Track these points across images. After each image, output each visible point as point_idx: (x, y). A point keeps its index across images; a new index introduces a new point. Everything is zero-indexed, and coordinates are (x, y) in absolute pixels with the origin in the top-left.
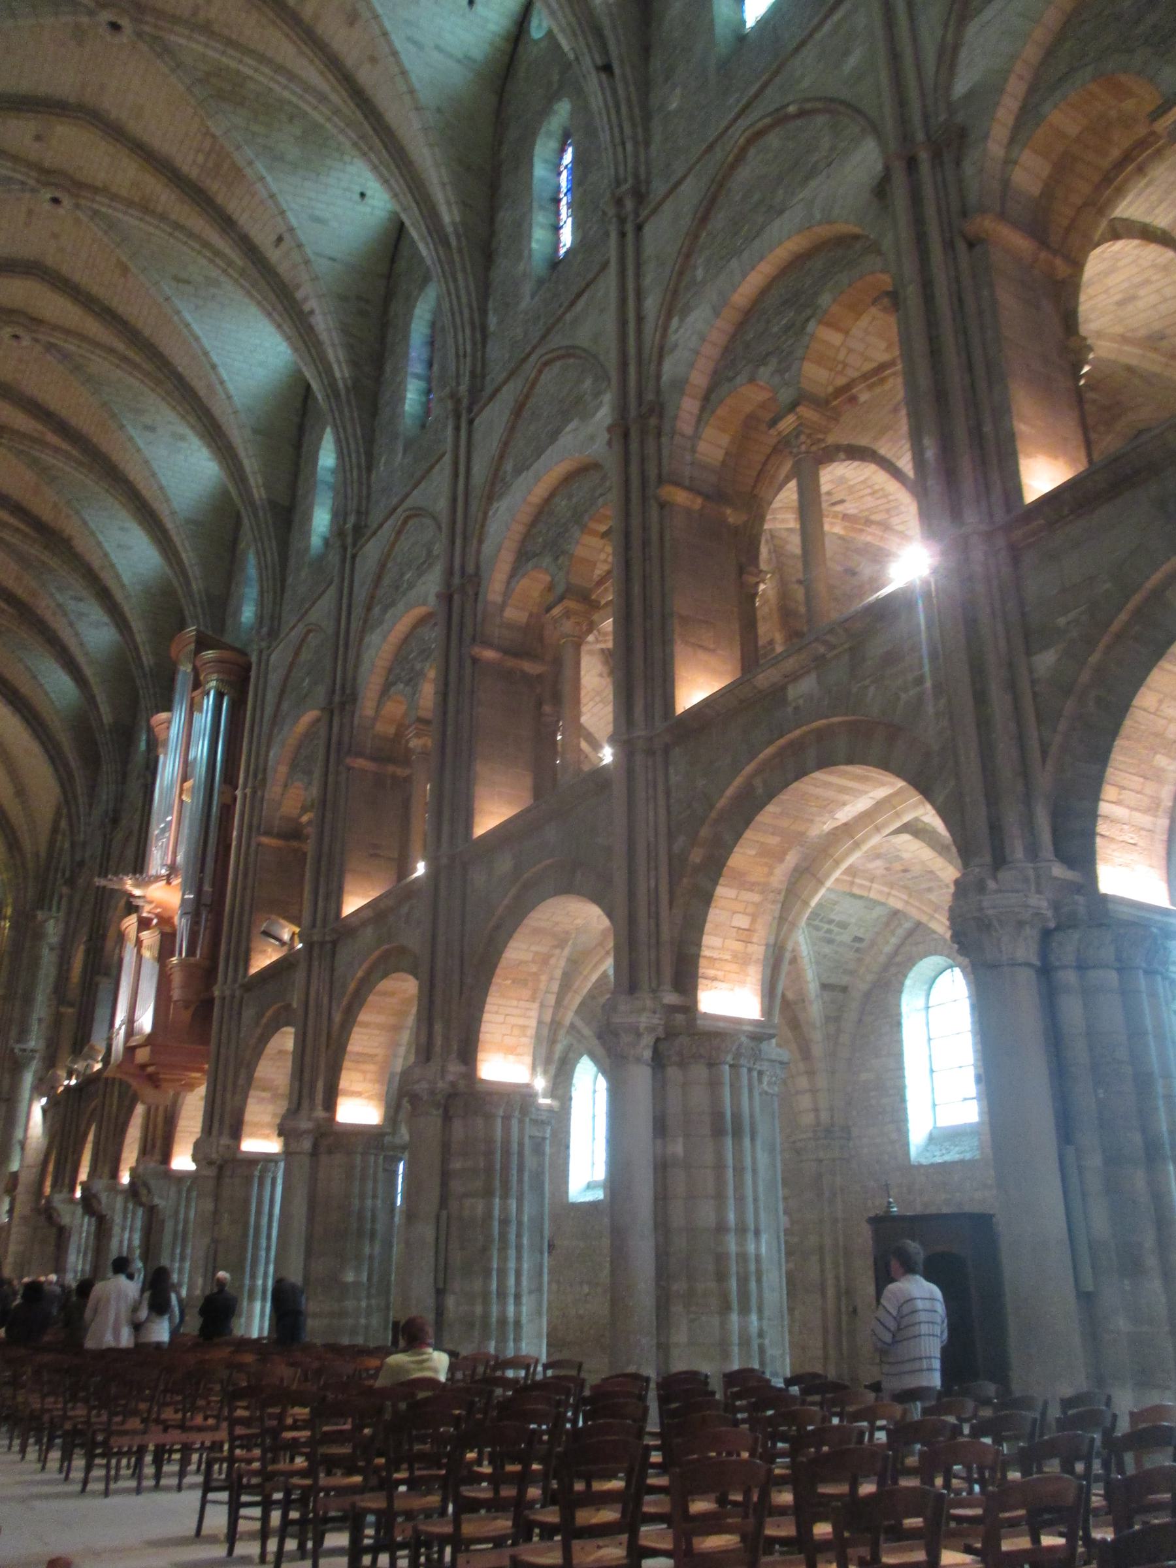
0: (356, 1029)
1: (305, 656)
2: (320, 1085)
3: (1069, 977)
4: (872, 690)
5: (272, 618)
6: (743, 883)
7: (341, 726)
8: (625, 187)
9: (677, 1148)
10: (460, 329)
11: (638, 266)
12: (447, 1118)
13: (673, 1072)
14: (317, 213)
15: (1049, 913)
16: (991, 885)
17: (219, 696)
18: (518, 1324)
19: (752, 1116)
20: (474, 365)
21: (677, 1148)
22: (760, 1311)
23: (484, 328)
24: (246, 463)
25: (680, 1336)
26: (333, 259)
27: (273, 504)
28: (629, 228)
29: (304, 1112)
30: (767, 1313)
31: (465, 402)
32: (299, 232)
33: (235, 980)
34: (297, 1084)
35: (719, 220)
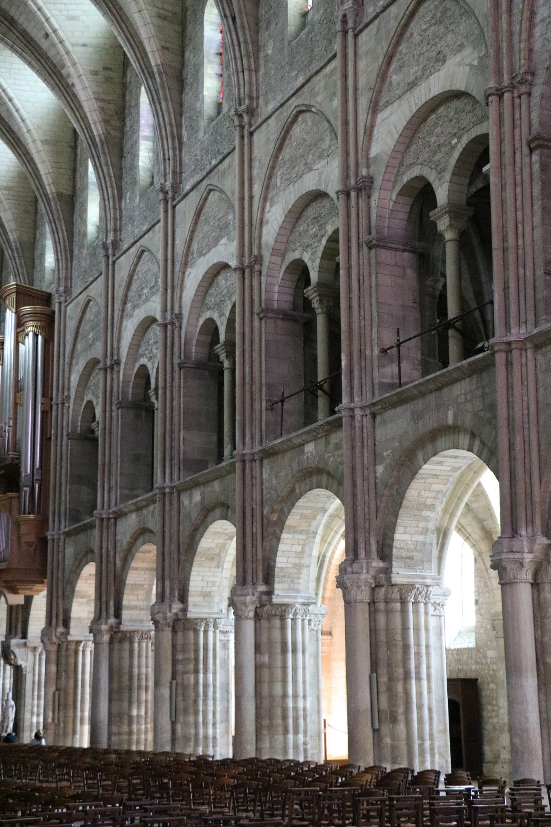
0: (130, 572)
1: (89, 316)
2: (112, 603)
3: (381, 606)
4: (331, 459)
5: (66, 278)
6: (294, 530)
7: (112, 379)
8: (243, 107)
9: (266, 659)
10: (165, 140)
11: (251, 160)
12: (174, 632)
13: (264, 623)
14: (71, 13)
15: (372, 581)
16: (349, 569)
17: (36, 335)
18: (214, 738)
19: (303, 642)
20: (175, 166)
21: (266, 659)
22: (305, 732)
24: (40, 166)
25: (266, 745)
26: (85, 45)
27: (60, 196)
28: (246, 134)
29: (103, 620)
30: (309, 734)
32: (60, 32)
33: (59, 529)
34: (99, 603)
35: (287, 153)
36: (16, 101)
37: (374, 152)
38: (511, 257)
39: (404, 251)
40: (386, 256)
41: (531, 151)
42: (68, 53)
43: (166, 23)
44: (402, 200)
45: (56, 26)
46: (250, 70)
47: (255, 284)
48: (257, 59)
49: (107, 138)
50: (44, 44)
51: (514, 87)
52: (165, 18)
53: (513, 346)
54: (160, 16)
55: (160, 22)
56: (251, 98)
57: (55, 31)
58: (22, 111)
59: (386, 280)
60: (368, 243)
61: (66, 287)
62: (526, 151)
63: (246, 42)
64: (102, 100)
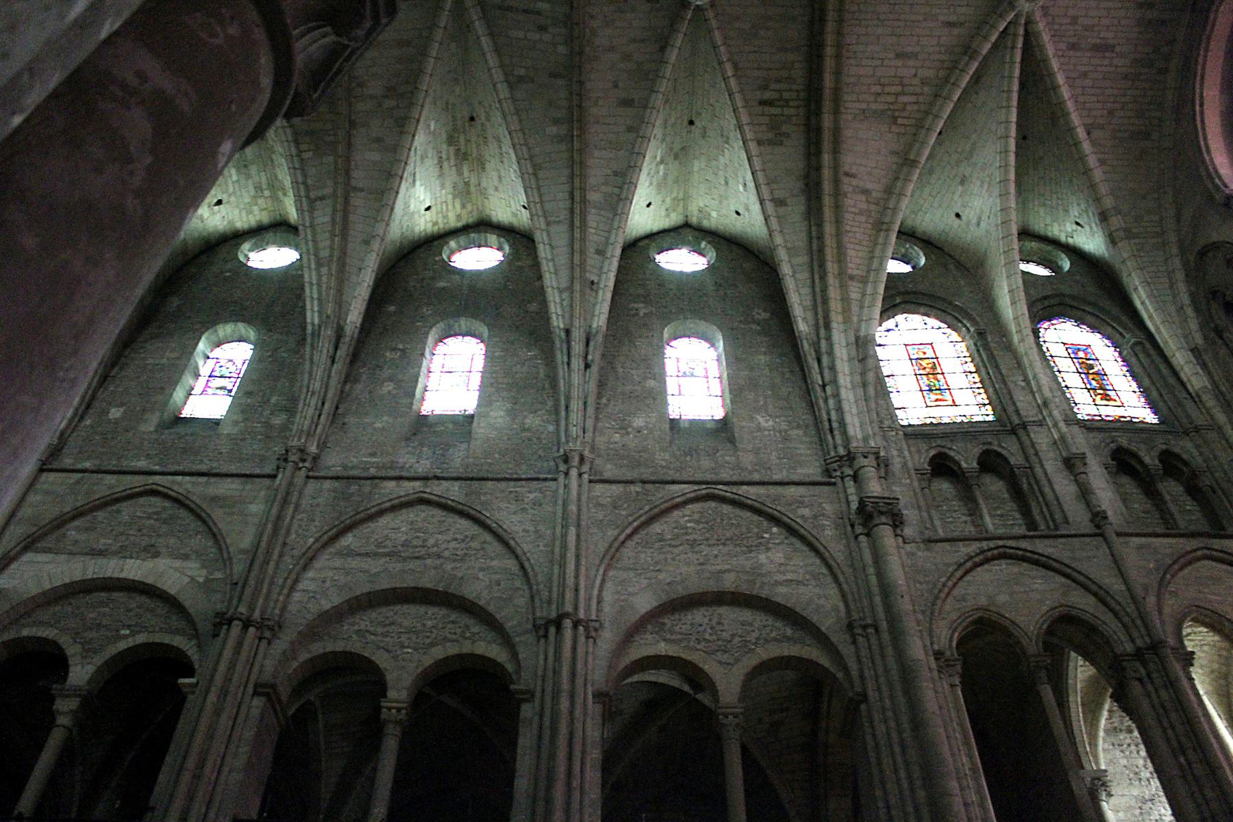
41: (256, 693)
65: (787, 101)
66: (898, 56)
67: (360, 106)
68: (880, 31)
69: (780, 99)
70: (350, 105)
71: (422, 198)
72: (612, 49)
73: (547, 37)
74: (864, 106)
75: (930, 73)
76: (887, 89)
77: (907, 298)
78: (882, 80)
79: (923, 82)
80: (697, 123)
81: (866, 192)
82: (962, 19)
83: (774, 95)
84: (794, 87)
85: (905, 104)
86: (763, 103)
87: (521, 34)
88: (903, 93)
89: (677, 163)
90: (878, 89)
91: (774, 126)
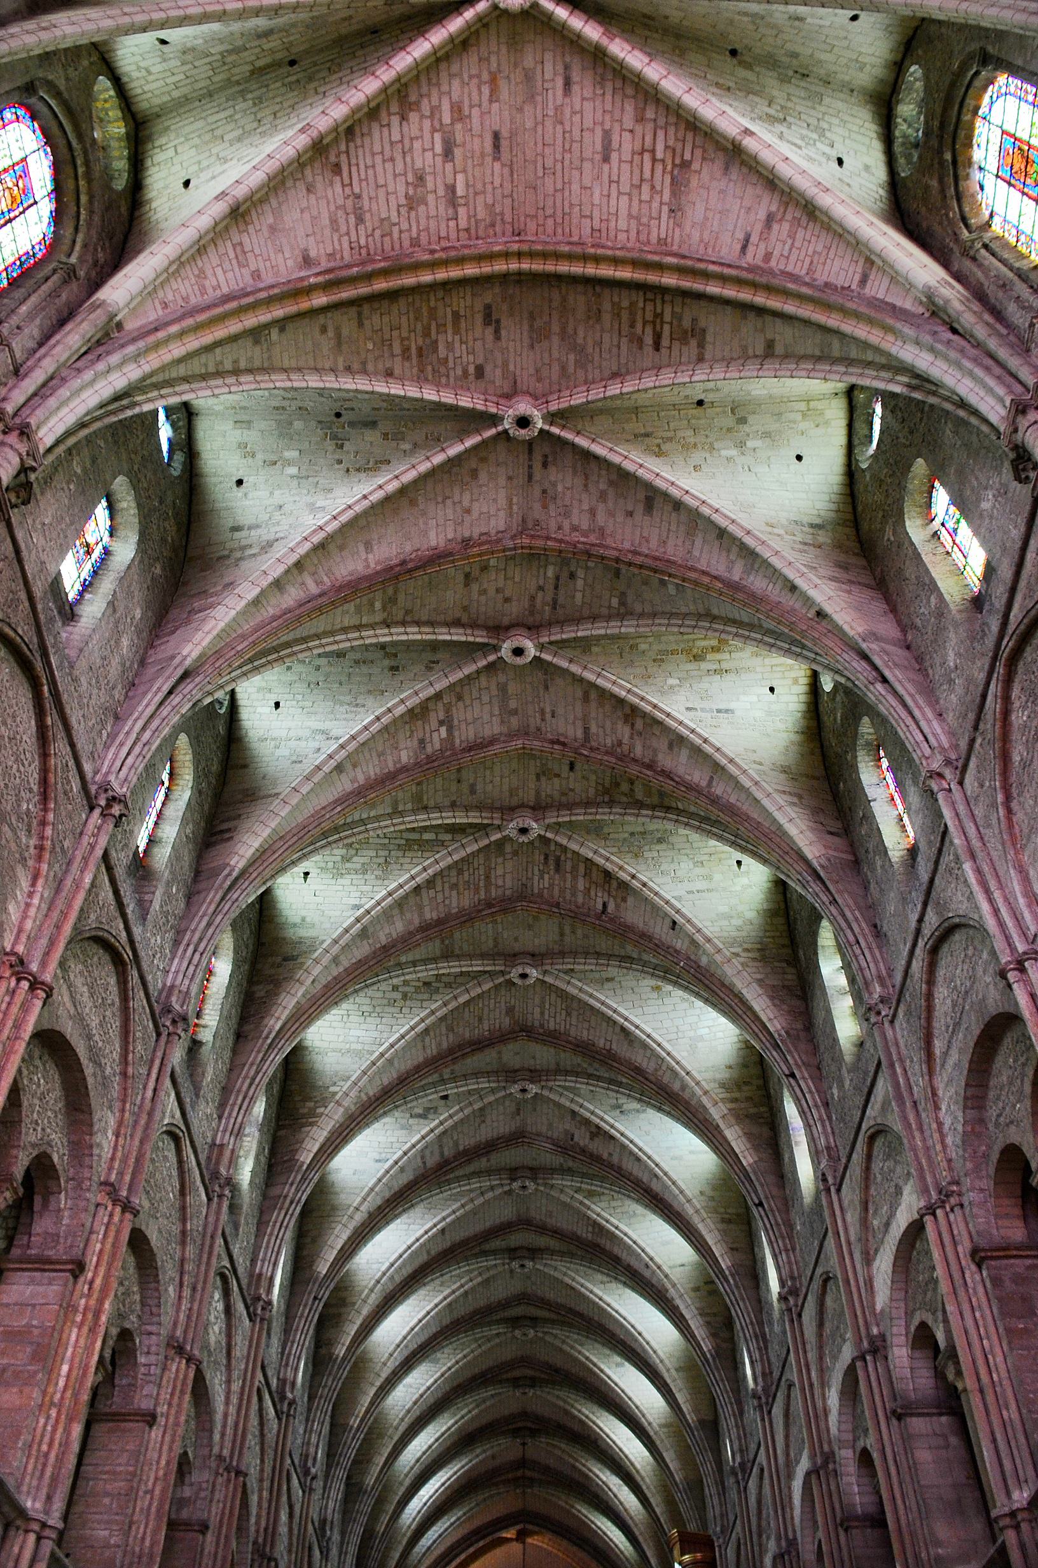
11: (804, 1344)
23: (764, 1335)
27: (702, 1422)
31: (763, 1400)
32: (657, 1259)
35: (827, 1330)
36: (645, 1334)
37: (878, 1307)
38: (990, 1398)
39: (941, 1414)
40: (917, 1424)
42: (666, 1276)
43: (732, 1226)
44: (917, 1354)
45: (652, 1254)
46: (787, 1250)
47: (833, 1488)
48: (791, 1238)
49: (718, 1352)
50: (647, 1274)
51: (943, 1202)
52: (730, 1221)
53: (1019, 1518)
54: (723, 1221)
55: (724, 1226)
56: (792, 1278)
57: (651, 1259)
58: (653, 1343)
59: (924, 1456)
60: (894, 1412)
61: (722, 1526)
62: (973, 1267)
63: (778, 1224)
64: (708, 1314)
65: (656, 315)
66: (606, 159)
67: (638, 751)
68: (575, 187)
69: (654, 323)
70: (635, 760)
71: (755, 698)
72: (593, 512)
73: (581, 573)
74: (665, 209)
75: (629, 108)
76: (647, 174)
77: (948, 139)
78: (636, 181)
79: (640, 119)
80: (702, 397)
81: (770, 219)
82: (560, 68)
83: (649, 330)
84: (641, 305)
85: (666, 147)
86: (657, 346)
87: (579, 595)
88: (653, 151)
89: (751, 419)
90: (646, 188)
91: (683, 336)
